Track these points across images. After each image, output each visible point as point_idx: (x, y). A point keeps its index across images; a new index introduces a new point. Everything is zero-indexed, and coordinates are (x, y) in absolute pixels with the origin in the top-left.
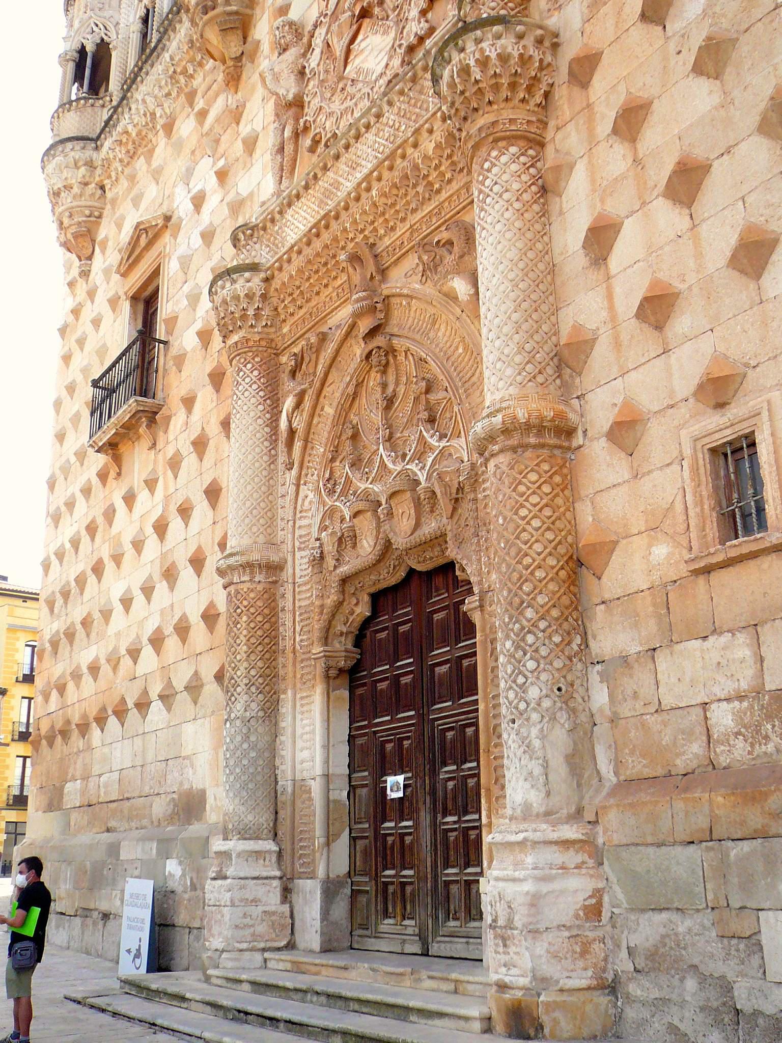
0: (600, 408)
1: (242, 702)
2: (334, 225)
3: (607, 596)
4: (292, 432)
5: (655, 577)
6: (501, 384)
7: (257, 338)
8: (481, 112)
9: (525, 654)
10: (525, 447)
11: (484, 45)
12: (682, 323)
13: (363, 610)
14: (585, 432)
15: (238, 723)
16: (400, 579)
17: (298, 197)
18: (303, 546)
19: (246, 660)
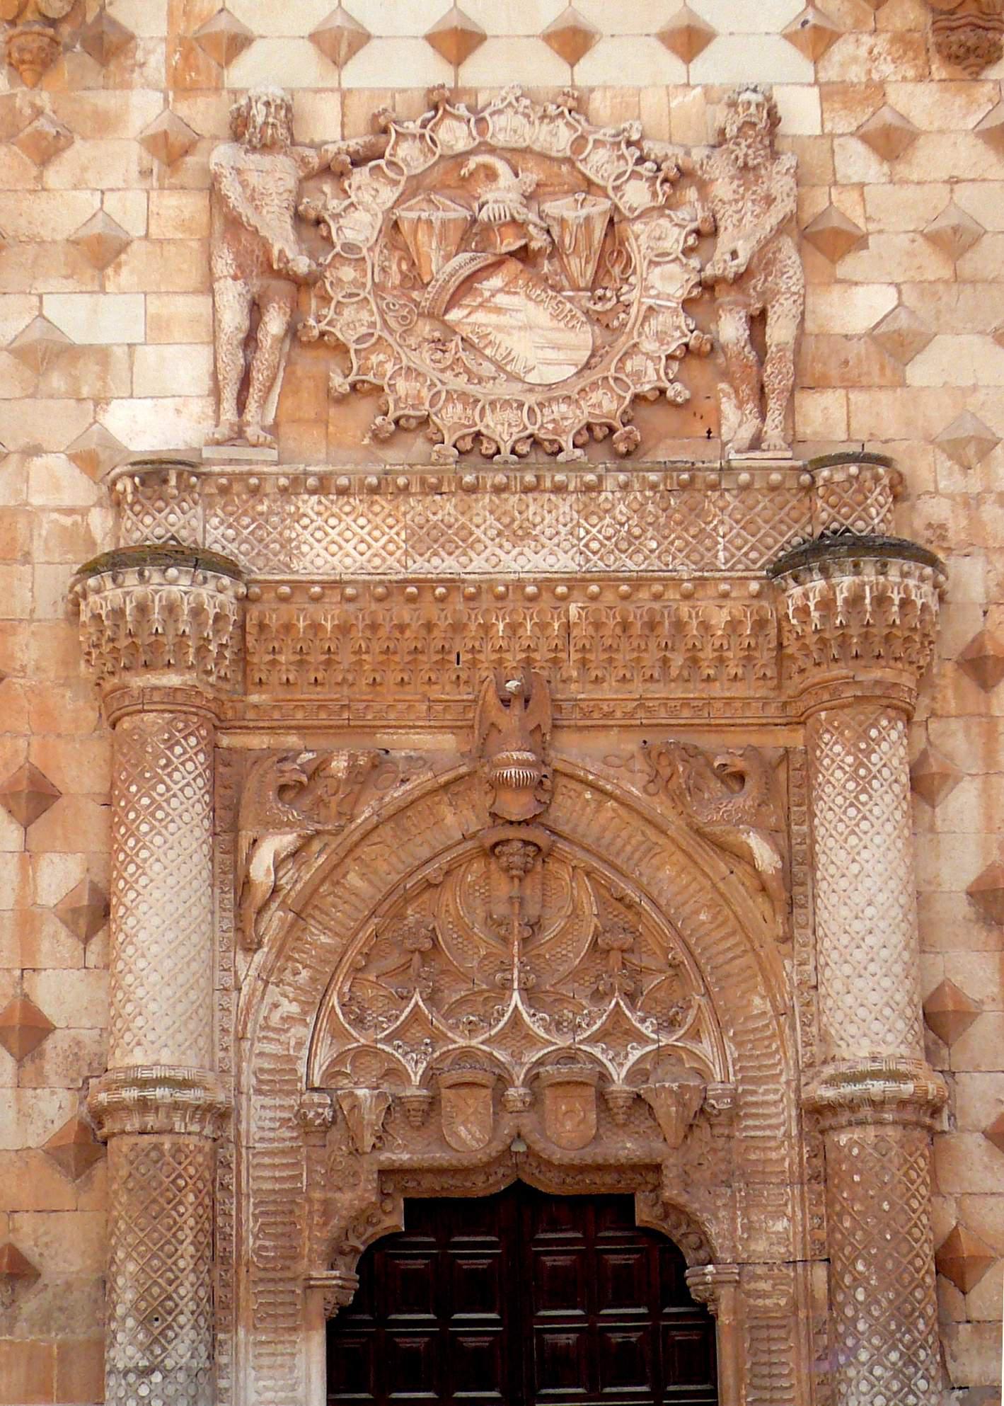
1: (187, 1342)
3: (975, 1315)
4: (275, 890)
6: (890, 1037)
8: (883, 663)
9: (916, 1373)
10: (918, 1124)
11: (912, 582)
13: (395, 1220)
14: (952, 1116)
15: (181, 1376)
17: (343, 492)
18: (266, 1088)
19: (193, 1271)
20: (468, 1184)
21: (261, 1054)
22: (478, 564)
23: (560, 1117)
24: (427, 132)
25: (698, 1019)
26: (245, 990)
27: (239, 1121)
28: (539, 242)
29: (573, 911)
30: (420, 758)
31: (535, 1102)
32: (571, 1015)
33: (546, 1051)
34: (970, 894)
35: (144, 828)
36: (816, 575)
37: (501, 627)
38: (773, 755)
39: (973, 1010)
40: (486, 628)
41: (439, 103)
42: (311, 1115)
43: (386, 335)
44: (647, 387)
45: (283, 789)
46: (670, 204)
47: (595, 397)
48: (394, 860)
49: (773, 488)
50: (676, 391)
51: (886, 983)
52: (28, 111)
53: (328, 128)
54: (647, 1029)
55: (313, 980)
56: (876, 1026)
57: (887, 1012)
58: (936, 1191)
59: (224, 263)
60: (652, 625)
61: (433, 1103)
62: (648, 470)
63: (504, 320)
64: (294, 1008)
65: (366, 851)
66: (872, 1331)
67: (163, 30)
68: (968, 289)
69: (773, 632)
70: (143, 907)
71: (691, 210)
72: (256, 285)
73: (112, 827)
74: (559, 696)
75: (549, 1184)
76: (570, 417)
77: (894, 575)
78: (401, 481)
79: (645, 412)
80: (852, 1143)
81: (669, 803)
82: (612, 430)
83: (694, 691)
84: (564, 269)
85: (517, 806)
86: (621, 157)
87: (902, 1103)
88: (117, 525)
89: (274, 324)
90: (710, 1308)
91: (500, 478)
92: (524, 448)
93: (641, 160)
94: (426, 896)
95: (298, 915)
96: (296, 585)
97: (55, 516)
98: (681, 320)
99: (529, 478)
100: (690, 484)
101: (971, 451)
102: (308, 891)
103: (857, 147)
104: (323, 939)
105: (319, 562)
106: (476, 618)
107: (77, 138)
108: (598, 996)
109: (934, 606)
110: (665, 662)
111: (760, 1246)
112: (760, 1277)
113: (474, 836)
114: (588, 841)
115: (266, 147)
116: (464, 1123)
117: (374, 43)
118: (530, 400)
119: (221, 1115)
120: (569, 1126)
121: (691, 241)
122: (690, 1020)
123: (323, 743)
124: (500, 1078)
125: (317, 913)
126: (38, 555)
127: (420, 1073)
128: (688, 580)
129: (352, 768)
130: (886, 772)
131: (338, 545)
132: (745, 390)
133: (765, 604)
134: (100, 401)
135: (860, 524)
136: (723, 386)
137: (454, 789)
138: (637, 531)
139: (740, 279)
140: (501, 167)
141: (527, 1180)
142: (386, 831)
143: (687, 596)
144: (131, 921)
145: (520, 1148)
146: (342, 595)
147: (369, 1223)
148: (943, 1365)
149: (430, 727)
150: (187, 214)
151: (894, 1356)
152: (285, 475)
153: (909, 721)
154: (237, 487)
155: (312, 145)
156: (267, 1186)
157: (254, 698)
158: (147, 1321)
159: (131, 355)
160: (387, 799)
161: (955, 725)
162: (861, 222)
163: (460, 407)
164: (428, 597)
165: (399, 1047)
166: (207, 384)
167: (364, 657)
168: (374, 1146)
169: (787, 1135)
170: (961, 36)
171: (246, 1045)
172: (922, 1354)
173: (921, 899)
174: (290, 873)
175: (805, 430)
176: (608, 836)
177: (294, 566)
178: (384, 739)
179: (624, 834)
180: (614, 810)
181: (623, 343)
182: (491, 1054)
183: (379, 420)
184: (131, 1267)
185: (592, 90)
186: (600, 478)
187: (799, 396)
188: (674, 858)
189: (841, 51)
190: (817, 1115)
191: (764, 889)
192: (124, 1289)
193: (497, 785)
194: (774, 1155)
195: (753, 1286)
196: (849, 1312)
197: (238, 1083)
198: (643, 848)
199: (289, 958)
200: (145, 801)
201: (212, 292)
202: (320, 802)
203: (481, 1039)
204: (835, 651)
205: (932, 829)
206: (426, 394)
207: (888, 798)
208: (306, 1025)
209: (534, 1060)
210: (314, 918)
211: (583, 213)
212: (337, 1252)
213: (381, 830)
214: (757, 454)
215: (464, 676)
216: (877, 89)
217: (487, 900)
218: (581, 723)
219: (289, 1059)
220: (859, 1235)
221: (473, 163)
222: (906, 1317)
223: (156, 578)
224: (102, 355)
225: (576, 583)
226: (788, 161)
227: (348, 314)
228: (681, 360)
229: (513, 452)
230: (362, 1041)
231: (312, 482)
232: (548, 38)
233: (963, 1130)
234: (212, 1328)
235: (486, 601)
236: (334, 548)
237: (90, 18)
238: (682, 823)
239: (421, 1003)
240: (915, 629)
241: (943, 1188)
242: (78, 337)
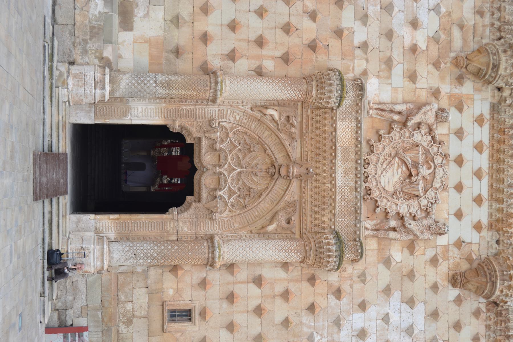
0: (215, 276)
2: (330, 158)
3: (164, 273)
4: (265, 115)
5: (165, 290)
6: (229, 256)
7: (311, 100)
10: (208, 262)
11: (333, 264)
12: (225, 305)
14: (210, 269)
15: (154, 90)
17: (357, 132)
21: (227, 111)
22: (339, 163)
24: (439, 154)
25: (233, 212)
26: (242, 107)
27: (212, 105)
28: (413, 179)
34: (261, 275)
35: (280, 84)
36: (335, 241)
38: (293, 230)
39: (235, 275)
40: (324, 165)
41: (446, 156)
43: (393, 143)
44: (379, 203)
45: (288, 117)
46: (421, 210)
47: (378, 192)
49: (355, 232)
50: (378, 210)
51: (241, 255)
52: (446, 61)
53: (441, 131)
54: (231, 200)
55: (244, 123)
56: (231, 253)
57: (235, 255)
58: (193, 265)
59: (410, 106)
60: (324, 203)
61: (216, 150)
62: (360, 203)
63: (395, 171)
64: (238, 119)
65: (274, 135)
66: (161, 250)
67: (464, 93)
68: (400, 278)
69: (322, 231)
70: (262, 84)
71: (420, 214)
72: (405, 113)
73: (280, 77)
75: (196, 176)
76: (372, 185)
77: (335, 259)
78: (359, 146)
79: (373, 202)
80: (204, 246)
81: (283, 206)
82: (369, 195)
83: (309, 213)
84: (406, 185)
85: (283, 172)
86: (433, 199)
87: (213, 258)
88: (350, 80)
89: (396, 117)
90: (167, 213)
91: (359, 169)
92: (366, 174)
93: (432, 203)
94: (263, 150)
95: (259, 120)
96: (335, 121)
97: (352, 66)
98: (394, 212)
99: (359, 176)
100: (357, 212)
101: (363, 278)
103: (434, 253)
105: (341, 126)
107: (439, 72)
108: (239, 189)
109: (327, 269)
110: (316, 206)
111: (181, 224)
112: (174, 224)
113: (276, 161)
114: (275, 187)
115: (437, 116)
117: (460, 142)
118: (377, 176)
119: (214, 101)
121: (413, 214)
122: (233, 210)
123: (298, 127)
124: (221, 166)
126: (343, 61)
130: (290, 256)
131: (344, 131)
132: (378, 226)
133: (329, 229)
134: (378, 77)
135: (347, 252)
136: (379, 221)
137: (287, 157)
138: (346, 200)
139: (404, 226)
140: (431, 171)
142: (278, 140)
143: (331, 211)
144: (259, 81)
145: (205, 170)
147: (188, 135)
148: (153, 266)
150: (421, 97)
151: (155, 255)
152: (361, 119)
153: (301, 262)
154: (358, 108)
155: (437, 127)
156: (197, 111)
157: (309, 111)
158: (168, 83)
159: (389, 84)
161: (300, 273)
162: (416, 254)
163: (375, 160)
164: (332, 151)
166: (382, 101)
169: (206, 231)
170: (459, 277)
171: (230, 107)
172: (156, 261)
173: (260, 264)
175: (368, 240)
177: (340, 120)
178: (299, 141)
179: (276, 196)
181: (389, 198)
183: (373, 141)
184: (180, 79)
185: (448, 192)
186: (359, 192)
187: (376, 238)
189: (456, 250)
190: (211, 239)
191: (263, 227)
192: (174, 78)
193: (288, 167)
194: (202, 228)
195: (172, 223)
196: (166, 245)
197: (221, 105)
199: (249, 118)
200: (286, 85)
201: (403, 103)
202: (285, 125)
204: (318, 245)
205: (276, 267)
206: (378, 152)
207: (284, 257)
211: (420, 189)
212: (182, 127)
214: (363, 228)
215: (313, 159)
216: (447, 258)
219: (226, 117)
220: (184, 247)
221: (432, 164)
222: (164, 257)
223: (338, 88)
224: (389, 77)
225: (335, 186)
226: (431, 237)
227: (398, 135)
228: (385, 211)
229: (365, 172)
231: (359, 125)
232: (460, 182)
233: (207, 272)
234: (165, 98)
235: (330, 165)
236: (344, 130)
237: (467, 76)
238: (278, 209)
240: (322, 264)
241: (193, 267)
242: (394, 71)
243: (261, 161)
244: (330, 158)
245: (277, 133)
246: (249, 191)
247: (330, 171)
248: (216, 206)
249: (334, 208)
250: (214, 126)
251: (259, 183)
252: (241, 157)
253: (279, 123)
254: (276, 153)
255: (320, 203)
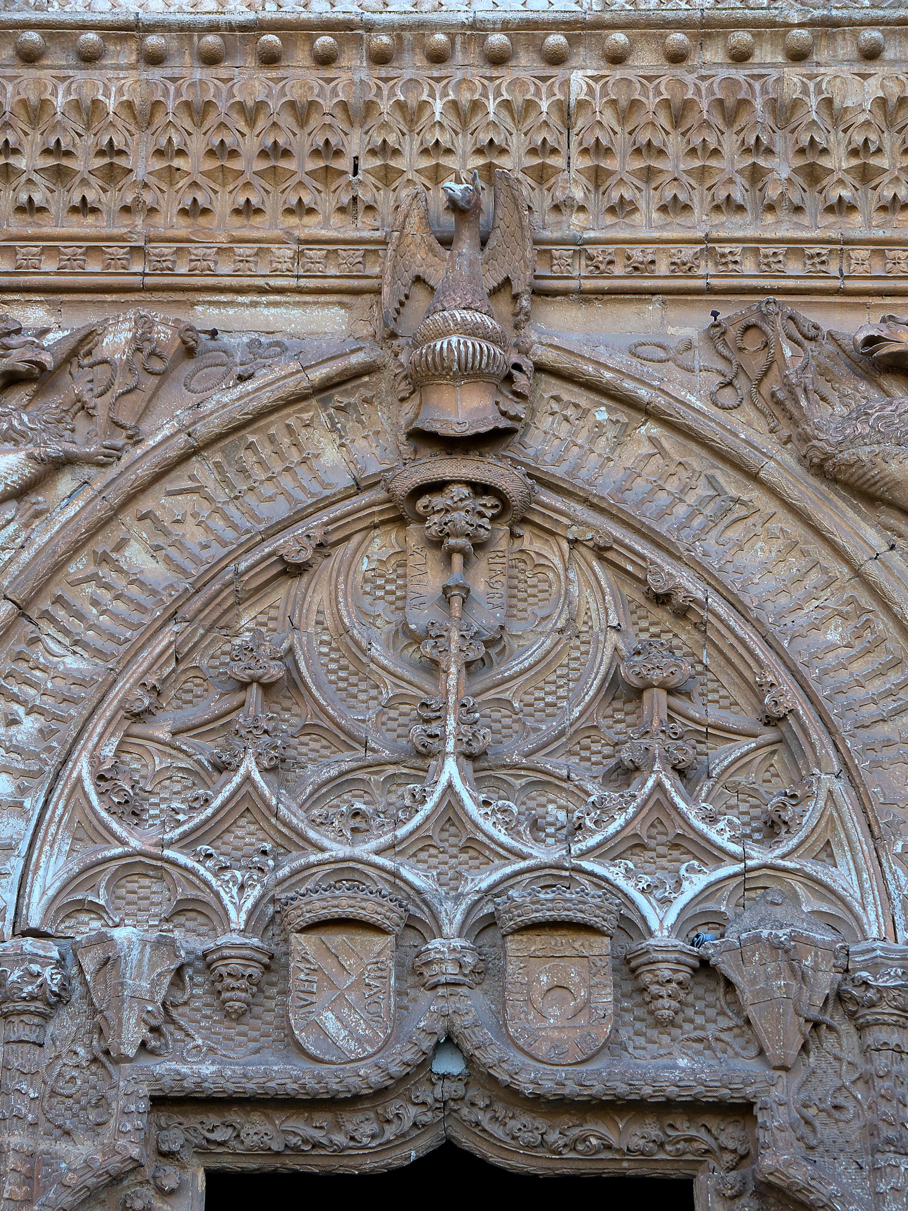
2: (354, 70)
16: (397, 1164)
20: (340, 1139)
23: (536, 996)
29: (567, 615)
30: (278, 344)
31: (484, 972)
32: (562, 816)
33: (508, 870)
37: (438, 106)
40: (411, 114)
42: (15, 975)
48: (218, 523)
60: (731, 111)
74: (547, 234)
75: (513, 1144)
81: (761, 425)
83: (816, 226)
85: (464, 409)
94: (279, 595)
95: (22, 610)
102: (46, 562)
104: (71, 662)
106: (392, 93)
108: (624, 773)
110: (756, 175)
114: (603, 488)
116: (333, 1006)
120: (555, 1014)
124: (411, 924)
125: (61, 614)
127: (249, 904)
128: (801, 25)
129: (141, 344)
141: (467, 1142)
143: (798, 56)
146: (140, 51)
149: (299, 291)
160: (209, 406)
165: (210, 856)
167: (178, 162)
168: (143, 1044)
174: (11, 528)
176: (640, 485)
178: (205, 315)
179: (672, 485)
180: (651, 439)
182: (396, 874)
188: (773, 525)
198: (708, 511)
203: (374, 844)
208: (24, 813)
209: (484, 885)
210: (52, 620)
213: (195, 466)
217: (400, 603)
218: (588, 284)
230: (135, 843)
239: (257, 776)
243: (380, 607)
244: (354, 70)
245: (144, 470)
246: (637, 693)
247: (467, 67)
248: (786, 953)
249: (772, 28)
250: (50, 976)
251: (567, 615)
252: (347, 760)
253: (54, 449)
254: (302, 488)
255: (730, 144)
